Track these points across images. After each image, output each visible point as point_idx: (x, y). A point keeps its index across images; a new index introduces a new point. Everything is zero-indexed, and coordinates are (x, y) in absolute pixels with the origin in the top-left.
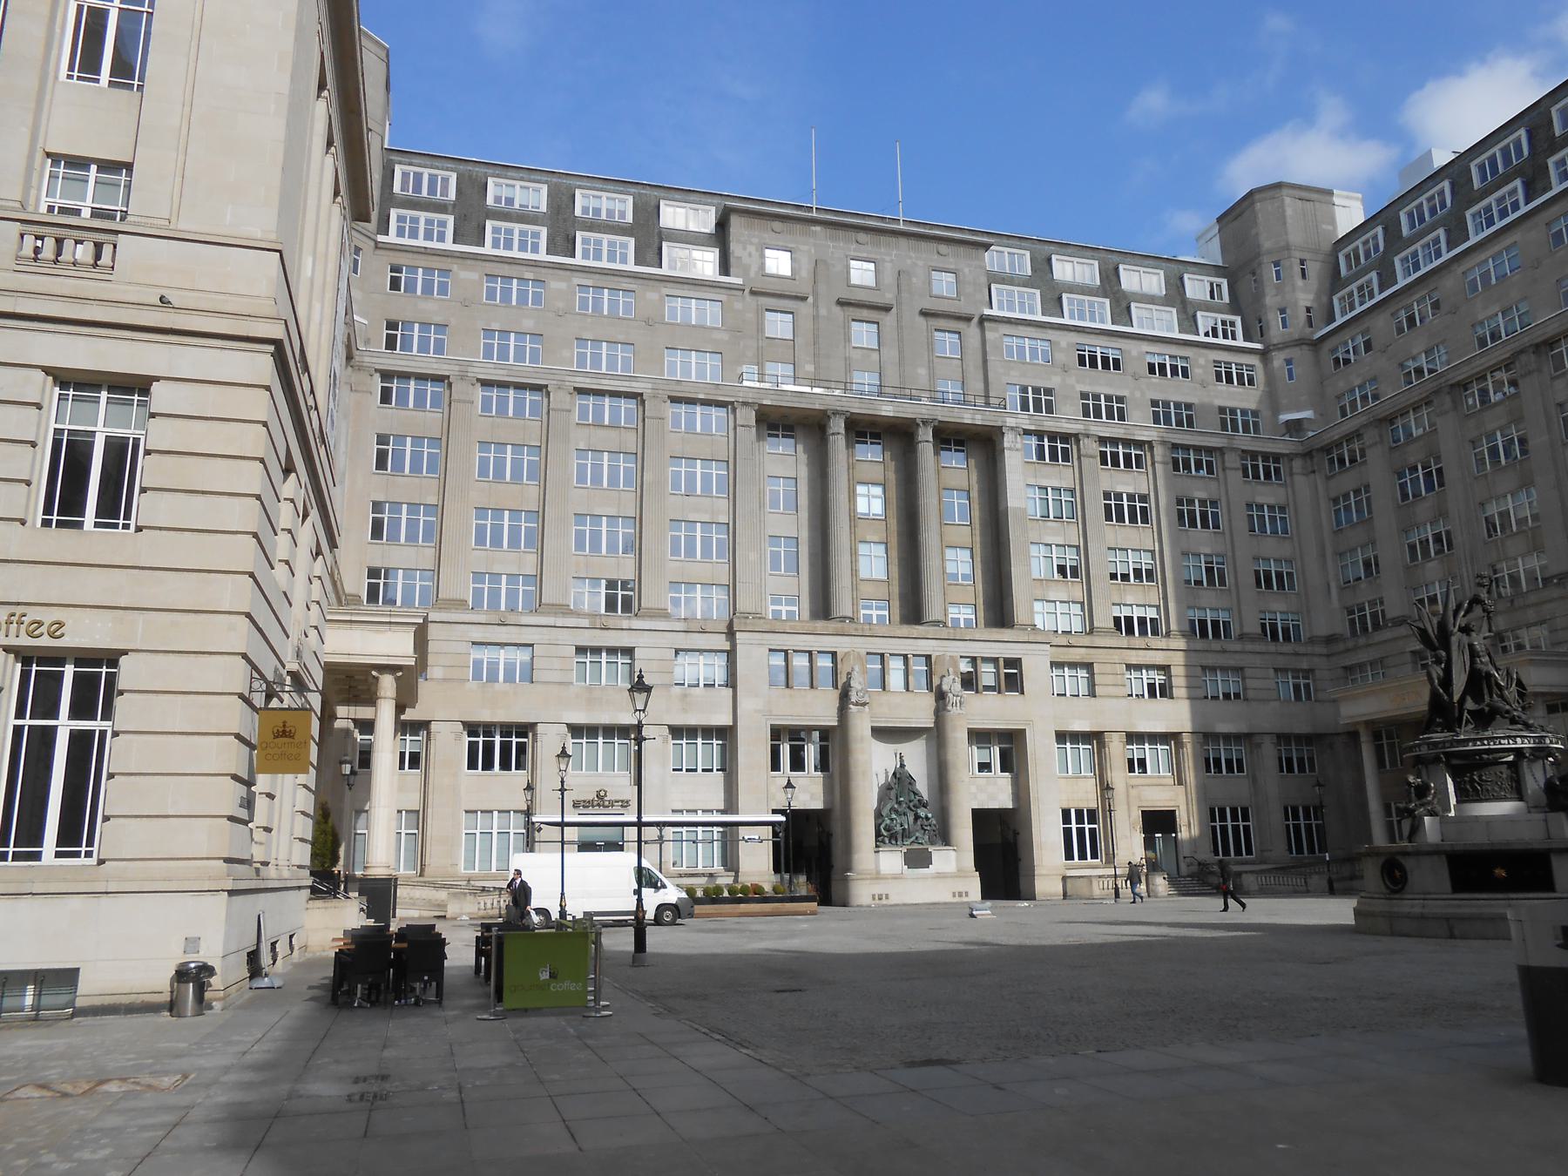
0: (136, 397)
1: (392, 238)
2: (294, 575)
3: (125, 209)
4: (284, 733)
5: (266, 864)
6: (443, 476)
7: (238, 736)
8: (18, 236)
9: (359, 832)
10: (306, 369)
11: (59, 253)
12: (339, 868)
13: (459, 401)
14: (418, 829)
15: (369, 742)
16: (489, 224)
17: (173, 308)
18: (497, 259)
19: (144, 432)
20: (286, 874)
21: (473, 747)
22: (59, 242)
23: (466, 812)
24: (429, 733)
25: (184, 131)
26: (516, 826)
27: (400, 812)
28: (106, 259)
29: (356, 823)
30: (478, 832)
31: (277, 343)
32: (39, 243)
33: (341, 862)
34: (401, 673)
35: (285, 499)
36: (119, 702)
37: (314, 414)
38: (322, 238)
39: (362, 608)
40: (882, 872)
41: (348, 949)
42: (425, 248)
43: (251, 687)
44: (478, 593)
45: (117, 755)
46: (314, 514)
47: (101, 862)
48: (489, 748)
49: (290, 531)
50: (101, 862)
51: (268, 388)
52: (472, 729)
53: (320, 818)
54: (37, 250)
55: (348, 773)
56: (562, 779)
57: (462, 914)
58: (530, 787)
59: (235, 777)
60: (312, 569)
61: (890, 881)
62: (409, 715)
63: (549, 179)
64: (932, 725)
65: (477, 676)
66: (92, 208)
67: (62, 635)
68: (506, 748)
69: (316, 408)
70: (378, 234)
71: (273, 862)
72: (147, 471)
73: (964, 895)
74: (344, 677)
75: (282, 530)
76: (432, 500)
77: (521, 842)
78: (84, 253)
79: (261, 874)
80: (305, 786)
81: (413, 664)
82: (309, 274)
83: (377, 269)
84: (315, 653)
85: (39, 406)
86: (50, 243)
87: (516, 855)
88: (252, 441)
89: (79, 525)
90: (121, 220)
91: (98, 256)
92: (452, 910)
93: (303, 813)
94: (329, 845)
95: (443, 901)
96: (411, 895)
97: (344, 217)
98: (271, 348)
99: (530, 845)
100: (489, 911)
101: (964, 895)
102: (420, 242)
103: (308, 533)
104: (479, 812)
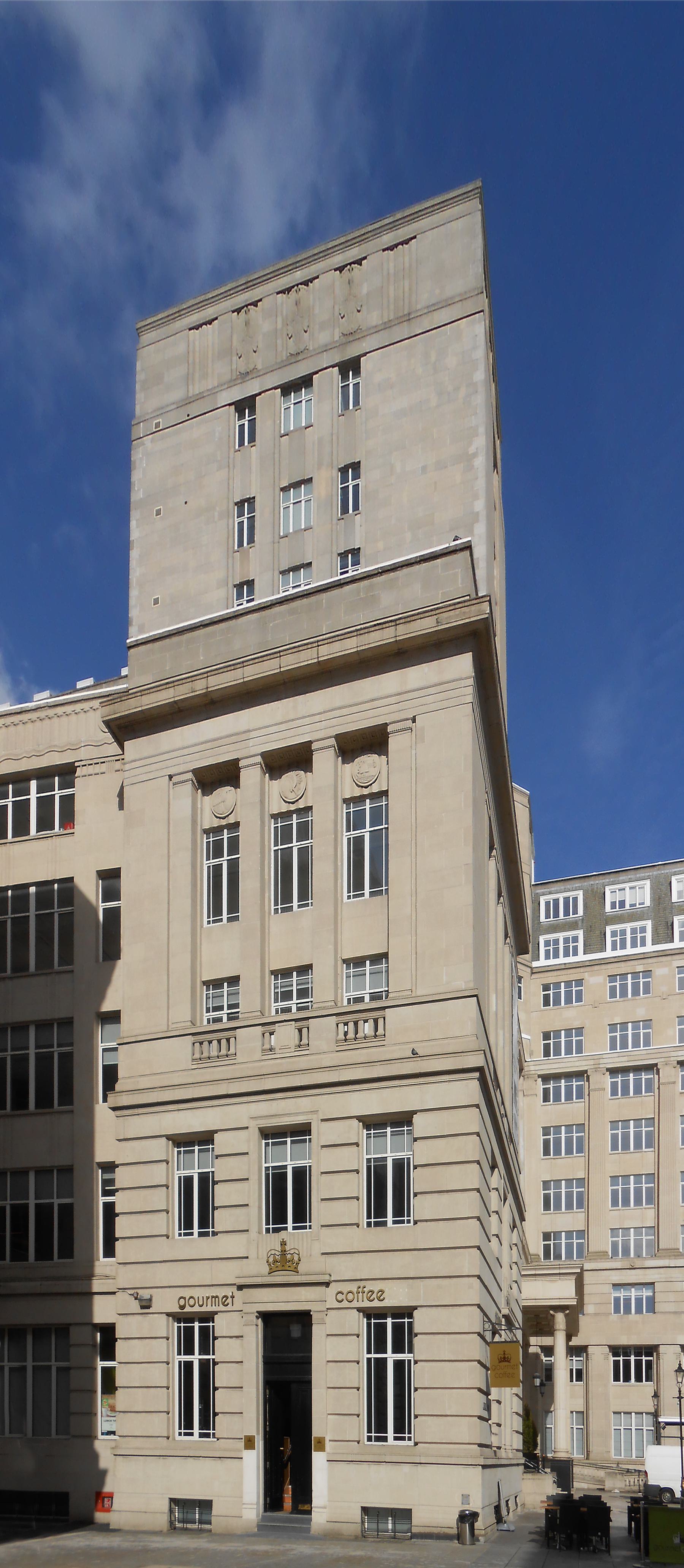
0: (406, 1128)
1: (542, 962)
2: (501, 1245)
3: (387, 989)
4: (504, 1359)
5: (499, 1448)
6: (587, 1154)
7: (479, 1362)
8: (335, 1026)
9: (548, 1426)
10: (499, 1086)
11: (356, 1033)
12: (538, 1451)
13: (595, 1090)
14: (584, 1425)
15: (550, 1362)
16: (609, 930)
17: (420, 1057)
18: (616, 960)
19: (412, 1153)
20: (511, 1456)
21: (616, 1364)
22: (356, 1024)
23: (614, 1413)
24: (587, 1355)
25: (414, 918)
26: (647, 1424)
27: (572, 1412)
28: (380, 1031)
29: (546, 1420)
30: (622, 1428)
31: (480, 1069)
32: (346, 1027)
33: (539, 1448)
34: (568, 1311)
35: (493, 1189)
36: (416, 1340)
37: (505, 1119)
38: (500, 975)
39: (541, 1264)
41: (552, 1509)
42: (565, 964)
43: (484, 1327)
44: (615, 1245)
45: (419, 1376)
46: (510, 1197)
47: (416, 1444)
48: (627, 1364)
49: (497, 1212)
50: (416, 1444)
51: (477, 1106)
52: (615, 1350)
53: (524, 1416)
54: (346, 1033)
55: (538, 1385)
56: (680, 1389)
57: (615, 1488)
58: (656, 1395)
59: (480, 1390)
60: (511, 1239)
62: (575, 1342)
63: (651, 874)
65: (617, 1310)
66: (370, 993)
67: (384, 1299)
68: (638, 1364)
69: (506, 1116)
70: (532, 961)
71: (503, 1447)
72: (418, 1180)
74: (533, 1316)
75: (493, 1212)
76: (581, 1175)
77: (651, 1437)
78: (367, 1028)
79: (497, 1455)
80: (517, 1395)
81: (576, 1303)
82: (495, 1010)
83: (533, 989)
84: (516, 1300)
85: (357, 1144)
86: (351, 1025)
87: (649, 1447)
88: (470, 1148)
89: (384, 1224)
90: (386, 998)
91: (376, 1029)
92: (608, 1485)
93: (517, 1413)
94: (531, 1434)
95: (602, 1478)
96: (582, 1472)
97: (512, 956)
98: (477, 1075)
99: (658, 1439)
100: (632, 1487)
102: (562, 960)
103: (507, 1212)
104: (622, 1413)
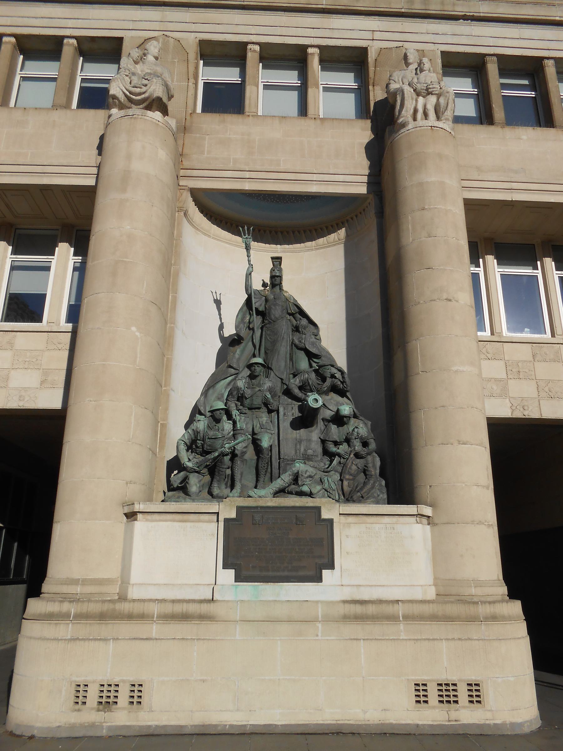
40: (134, 593)
61: (154, 629)
64: (363, 190)
73: (463, 694)
101: (463, 694)
